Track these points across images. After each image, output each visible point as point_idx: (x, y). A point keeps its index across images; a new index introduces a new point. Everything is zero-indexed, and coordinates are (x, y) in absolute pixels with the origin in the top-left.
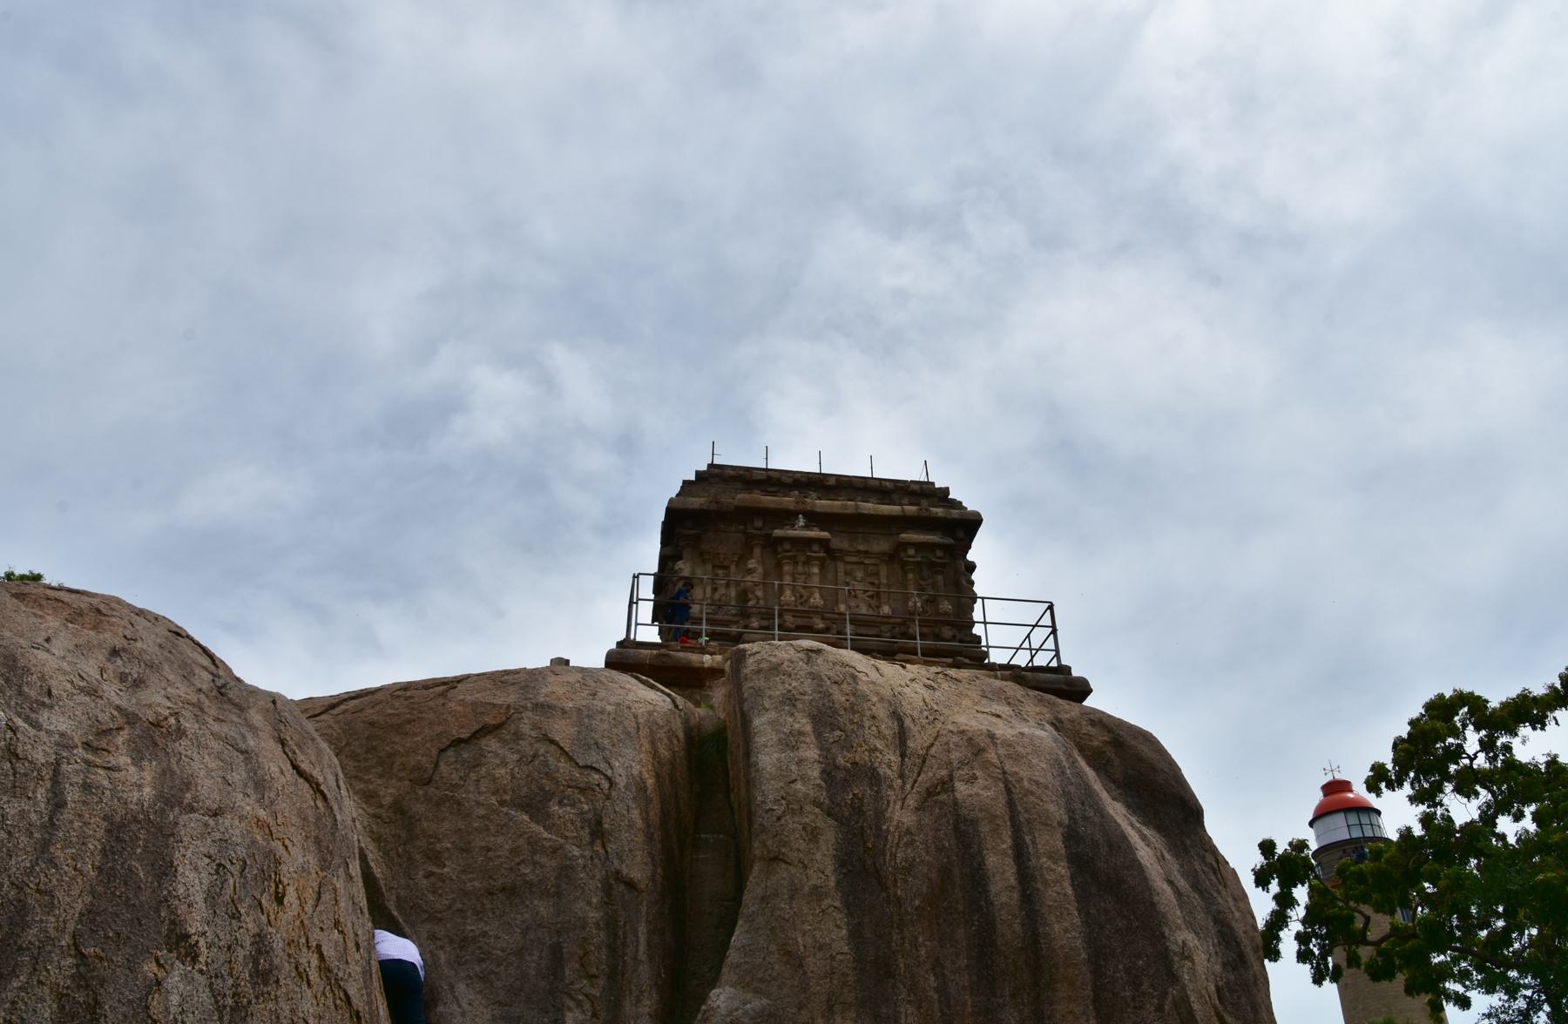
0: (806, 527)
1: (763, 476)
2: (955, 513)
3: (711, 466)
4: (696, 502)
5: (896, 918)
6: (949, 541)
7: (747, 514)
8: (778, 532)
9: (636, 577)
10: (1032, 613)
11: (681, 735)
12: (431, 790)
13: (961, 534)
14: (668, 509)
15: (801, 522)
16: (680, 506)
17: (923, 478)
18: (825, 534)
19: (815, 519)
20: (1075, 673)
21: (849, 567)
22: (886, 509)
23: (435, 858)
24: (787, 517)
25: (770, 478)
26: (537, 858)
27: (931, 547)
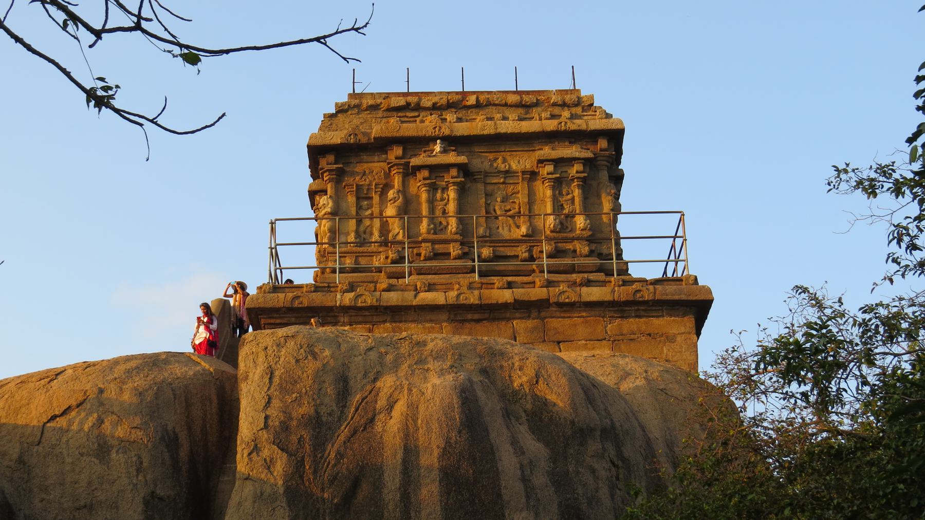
0: (444, 151)
1: (401, 102)
2: (596, 124)
3: (353, 95)
4: (336, 138)
5: (321, 511)
6: (589, 154)
7: (382, 145)
8: (415, 161)
9: (272, 223)
10: (668, 225)
11: (214, 398)
12: (40, 448)
13: (603, 143)
14: (308, 146)
15: (438, 148)
16: (320, 142)
17: (568, 86)
18: (462, 159)
19: (453, 142)
20: (701, 282)
21: (490, 188)
22: (527, 127)
23: (45, 489)
24: (422, 142)
25: (408, 104)
26: (104, 486)
27: (571, 161)
